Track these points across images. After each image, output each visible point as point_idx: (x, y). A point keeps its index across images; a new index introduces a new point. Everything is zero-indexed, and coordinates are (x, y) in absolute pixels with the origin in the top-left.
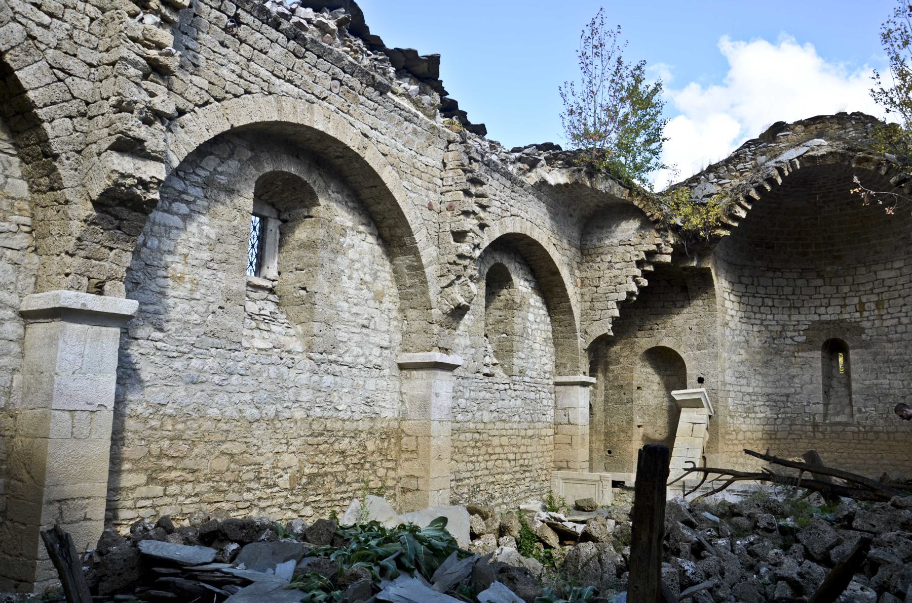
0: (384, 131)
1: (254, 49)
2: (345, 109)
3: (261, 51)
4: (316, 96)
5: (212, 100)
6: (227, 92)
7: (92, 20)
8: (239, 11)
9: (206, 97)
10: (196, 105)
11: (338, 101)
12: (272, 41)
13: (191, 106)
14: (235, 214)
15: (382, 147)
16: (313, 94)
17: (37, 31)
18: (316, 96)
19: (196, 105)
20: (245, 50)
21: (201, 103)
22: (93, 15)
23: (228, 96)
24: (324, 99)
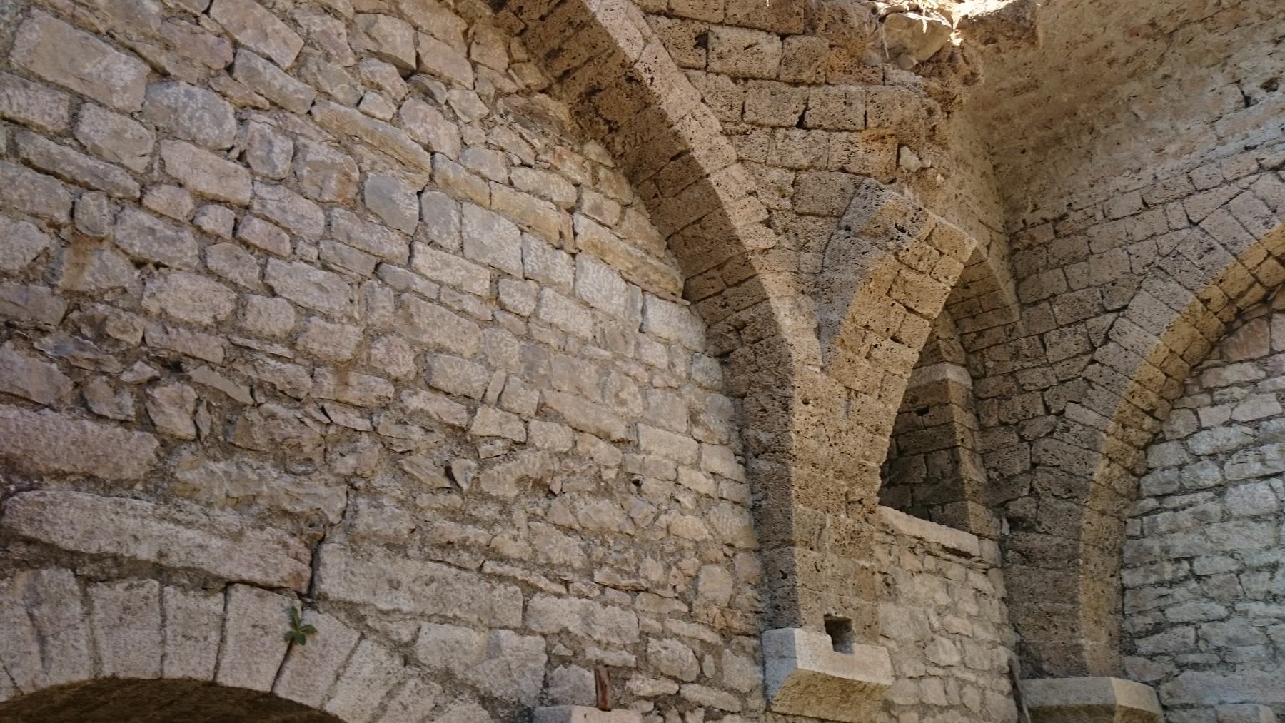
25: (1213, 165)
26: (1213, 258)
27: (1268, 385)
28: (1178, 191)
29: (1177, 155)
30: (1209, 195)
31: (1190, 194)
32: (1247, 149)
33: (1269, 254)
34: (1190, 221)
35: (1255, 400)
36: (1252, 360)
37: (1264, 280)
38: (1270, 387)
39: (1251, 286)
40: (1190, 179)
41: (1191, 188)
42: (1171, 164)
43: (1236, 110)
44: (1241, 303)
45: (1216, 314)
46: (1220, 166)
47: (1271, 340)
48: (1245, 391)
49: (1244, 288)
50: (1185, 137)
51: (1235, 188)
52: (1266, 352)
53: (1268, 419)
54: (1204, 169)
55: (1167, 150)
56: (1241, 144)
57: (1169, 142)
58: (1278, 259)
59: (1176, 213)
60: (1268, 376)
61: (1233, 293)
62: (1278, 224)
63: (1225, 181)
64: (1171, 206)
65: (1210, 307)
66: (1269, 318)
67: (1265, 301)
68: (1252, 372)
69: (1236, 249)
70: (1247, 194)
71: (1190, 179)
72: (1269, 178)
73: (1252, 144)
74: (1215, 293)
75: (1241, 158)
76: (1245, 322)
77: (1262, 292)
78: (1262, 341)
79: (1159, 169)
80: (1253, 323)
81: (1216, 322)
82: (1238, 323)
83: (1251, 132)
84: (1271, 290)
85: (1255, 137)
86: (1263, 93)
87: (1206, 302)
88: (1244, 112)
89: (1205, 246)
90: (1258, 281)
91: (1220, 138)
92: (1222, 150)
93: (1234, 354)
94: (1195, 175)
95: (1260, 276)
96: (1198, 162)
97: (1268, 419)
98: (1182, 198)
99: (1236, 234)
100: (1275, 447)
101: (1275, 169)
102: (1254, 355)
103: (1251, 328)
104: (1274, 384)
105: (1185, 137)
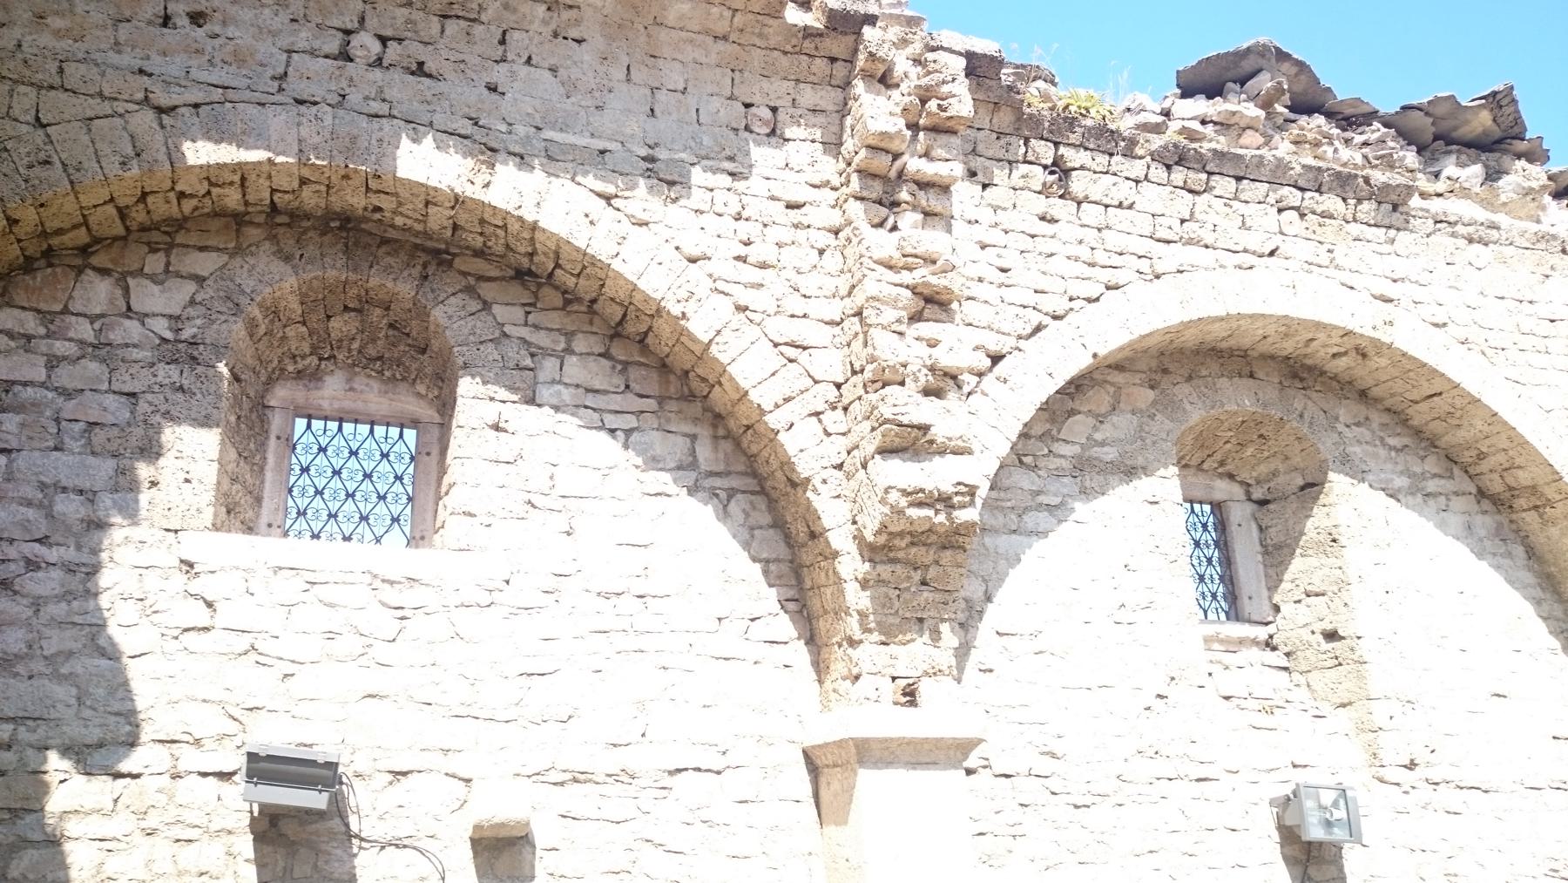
0: (1424, 278)
1: (1107, 206)
2: (1324, 259)
3: (1120, 206)
4: (1254, 253)
5: (1047, 320)
6: (1071, 299)
7: (821, 252)
8: (1062, 150)
9: (1036, 318)
10: (1020, 337)
11: (1299, 250)
12: (1137, 182)
13: (1012, 342)
14: (1142, 524)
15: (1427, 312)
16: (1245, 251)
17: (745, 297)
18: (1254, 253)
19: (1020, 337)
20: (1091, 213)
21: (1029, 331)
22: (820, 245)
23: (1076, 304)
24: (1272, 254)
25: (95, 69)
26: (44, 174)
27: (43, 346)
28: (40, 76)
29: (58, 34)
30: (74, 100)
31: (52, 87)
32: (141, 71)
33: (112, 200)
34: (38, 119)
35: (20, 358)
36: (38, 311)
37: (94, 227)
38: (44, 349)
39: (75, 227)
40: (61, 71)
41: (57, 81)
42: (46, 39)
43: (150, 23)
44: (55, 241)
45: (19, 241)
46: (103, 74)
47: (70, 297)
48: (13, 344)
49: (66, 225)
50: (78, 19)
51: (107, 108)
52: (58, 307)
53: (25, 384)
54: (83, 67)
55: (49, 20)
56: (137, 63)
57: (57, 13)
58: (119, 210)
59: (25, 100)
60: (48, 336)
61: (52, 225)
62: (135, 171)
63: (101, 94)
64: (22, 89)
65: (15, 229)
66: (80, 271)
67: (84, 250)
68: (31, 324)
69: (76, 176)
70: (118, 121)
71: (61, 71)
72: (149, 116)
73: (148, 69)
74: (29, 216)
75: (130, 77)
76: (50, 265)
77: (87, 240)
78: (59, 294)
79: (29, 38)
80: (59, 270)
81: (15, 251)
82: (42, 263)
83: (154, 56)
84: (97, 240)
85: (156, 64)
86: (186, 21)
87: (12, 222)
88: (158, 30)
89: (42, 156)
90: (86, 224)
91: (117, 43)
92: (113, 58)
93: (20, 297)
94: (70, 68)
95: (91, 220)
96: (81, 55)
97: (25, 384)
98: (40, 87)
99: (83, 159)
100: (18, 418)
101: (160, 110)
102: (43, 306)
103: (54, 274)
104: (50, 347)
105: (78, 19)
